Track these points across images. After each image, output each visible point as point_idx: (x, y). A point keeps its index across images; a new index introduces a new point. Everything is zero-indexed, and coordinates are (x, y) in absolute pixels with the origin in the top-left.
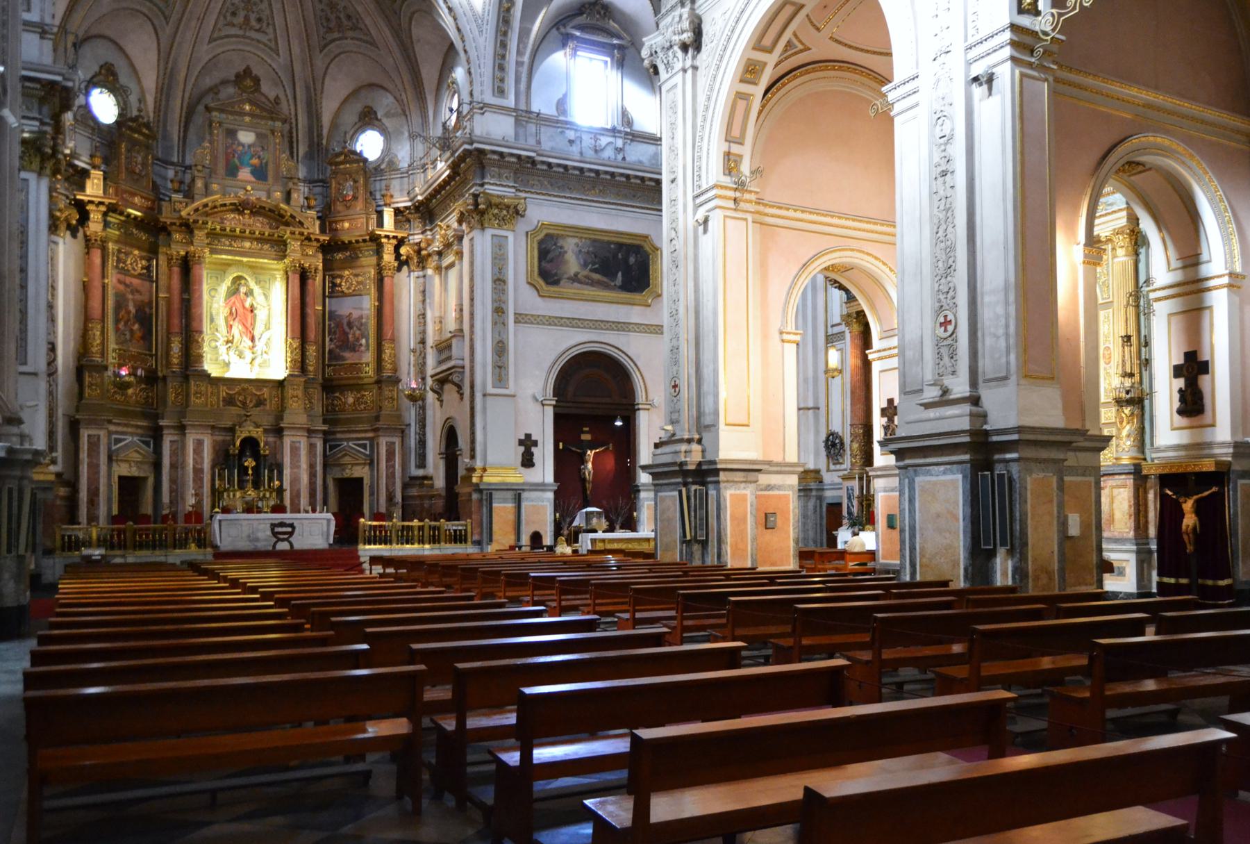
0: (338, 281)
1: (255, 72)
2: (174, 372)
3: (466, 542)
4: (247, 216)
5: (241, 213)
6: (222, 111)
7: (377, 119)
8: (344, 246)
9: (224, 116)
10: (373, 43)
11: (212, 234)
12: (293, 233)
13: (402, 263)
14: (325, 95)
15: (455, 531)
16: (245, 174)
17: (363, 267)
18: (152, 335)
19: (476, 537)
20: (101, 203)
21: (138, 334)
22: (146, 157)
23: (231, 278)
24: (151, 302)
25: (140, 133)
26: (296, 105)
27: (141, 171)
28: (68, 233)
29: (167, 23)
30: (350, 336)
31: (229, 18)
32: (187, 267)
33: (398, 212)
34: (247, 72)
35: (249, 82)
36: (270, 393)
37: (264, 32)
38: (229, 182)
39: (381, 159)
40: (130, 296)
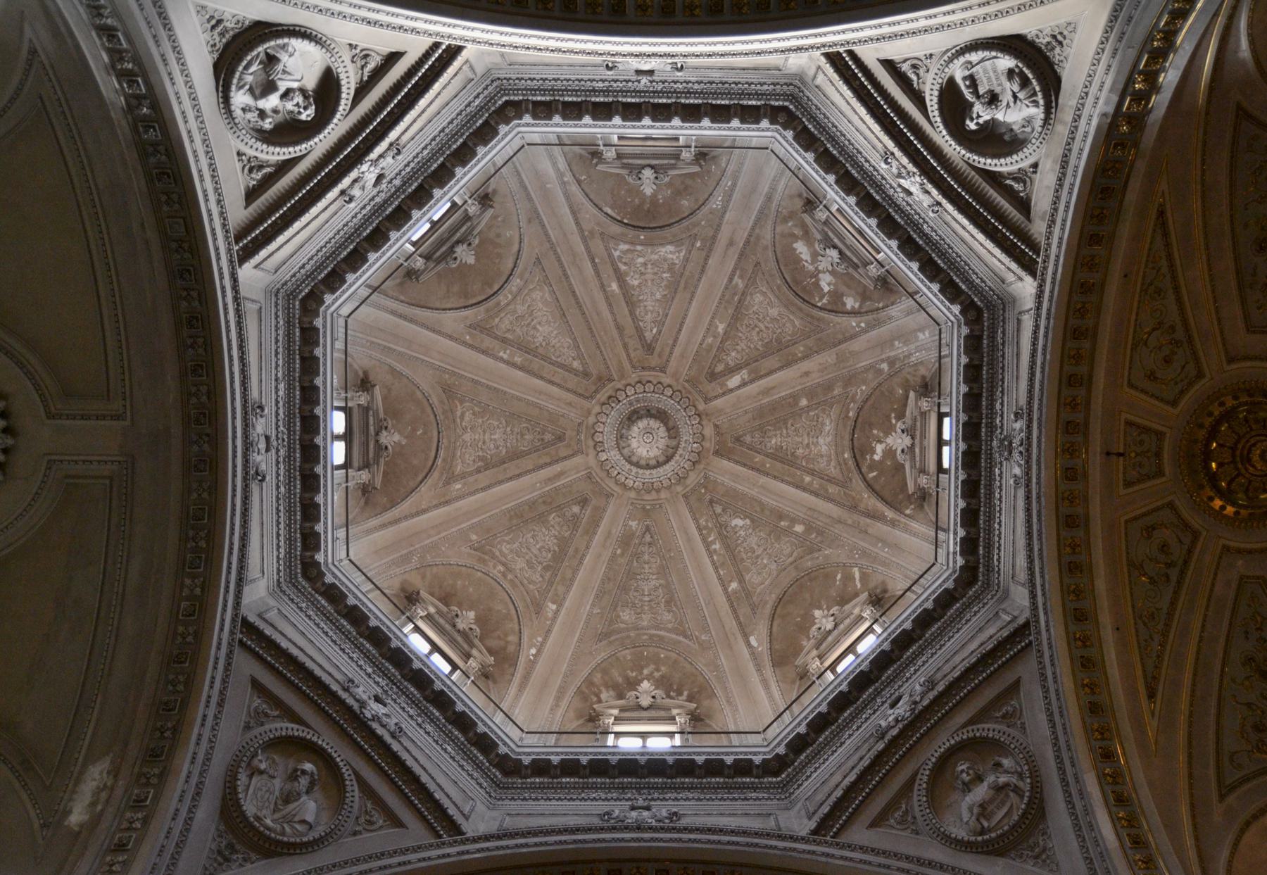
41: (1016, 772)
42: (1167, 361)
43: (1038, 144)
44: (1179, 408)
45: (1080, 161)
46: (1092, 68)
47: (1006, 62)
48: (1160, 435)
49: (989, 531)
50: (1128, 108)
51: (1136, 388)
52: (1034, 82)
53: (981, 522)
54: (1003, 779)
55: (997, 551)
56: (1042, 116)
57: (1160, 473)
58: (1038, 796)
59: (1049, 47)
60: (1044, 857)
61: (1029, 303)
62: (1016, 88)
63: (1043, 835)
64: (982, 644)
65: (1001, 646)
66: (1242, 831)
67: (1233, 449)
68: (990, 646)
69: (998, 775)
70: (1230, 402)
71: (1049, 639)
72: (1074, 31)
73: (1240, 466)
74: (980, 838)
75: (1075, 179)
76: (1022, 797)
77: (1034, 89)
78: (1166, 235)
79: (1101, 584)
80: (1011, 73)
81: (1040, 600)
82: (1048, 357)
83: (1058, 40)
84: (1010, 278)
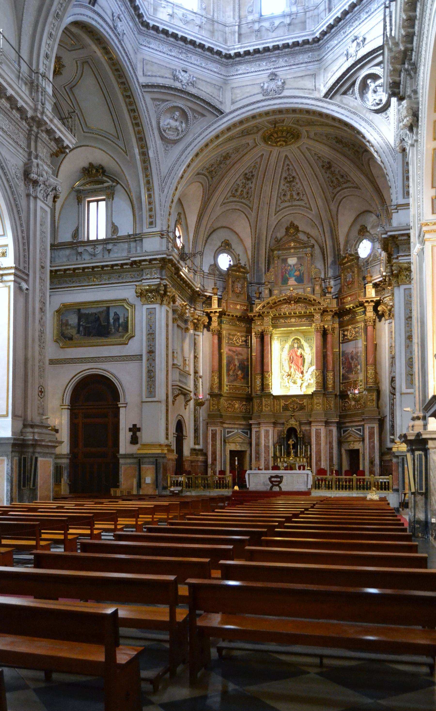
0: (346, 333)
1: (296, 223)
2: (257, 394)
3: (332, 489)
4: (293, 305)
5: (290, 303)
6: (279, 250)
7: (367, 231)
8: (349, 311)
9: (280, 252)
10: (357, 188)
11: (275, 318)
12: (315, 310)
13: (380, 316)
14: (339, 226)
15: (381, 482)
16: (292, 282)
17: (358, 322)
18: (248, 375)
19: (395, 487)
20: (216, 312)
21: (241, 376)
22: (243, 284)
23: (291, 340)
24: (248, 359)
25: (240, 272)
27: (240, 291)
28: (205, 329)
29: (252, 211)
30: (353, 365)
31: (282, 198)
32: (262, 337)
33: (376, 286)
34: (292, 225)
35: (292, 231)
36: (307, 402)
38: (284, 288)
39: (370, 255)
40: (236, 357)
62: (377, 101)
76: (177, 136)
80: (381, 100)
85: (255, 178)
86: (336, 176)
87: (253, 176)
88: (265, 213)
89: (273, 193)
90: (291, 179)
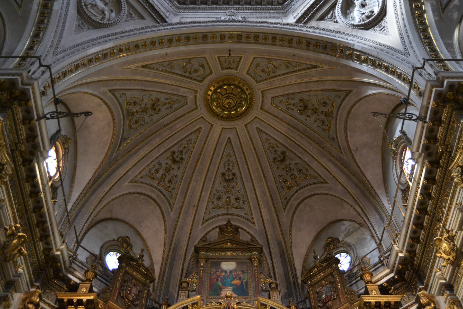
26: (272, 259)
31: (216, 202)
37: (241, 208)
41: (110, 18)
42: (263, 71)
43: (345, 23)
44: (246, 75)
45: (337, 37)
46: (371, 41)
47: (376, 10)
48: (236, 69)
49: (199, 9)
50: (355, 54)
51: (253, 60)
52: (368, 21)
53: (203, 6)
54: (107, 13)
55: (192, 11)
56: (355, 24)
57: (223, 69)
58: (102, 26)
59: (380, 26)
60: (80, 28)
61: (285, 21)
62: (366, 14)
63: (88, 28)
64: (157, 5)
65: (157, 12)
66: (99, 97)
67: (232, 93)
68: (156, 8)
69: (108, 11)
70: (247, 92)
71: (161, 30)
72: (385, 34)
73: (226, 96)
74: (83, 4)
75: (331, 36)
76: (101, 20)
77: (365, 21)
78: (308, 69)
79: (182, 48)
80: (372, 12)
81: (176, 26)
82: (266, 28)
83: (382, 29)
84: (295, 14)
85: (185, 162)
86: (292, 172)
87: (182, 159)
88: (190, 219)
89: (203, 193)
90: (230, 177)
